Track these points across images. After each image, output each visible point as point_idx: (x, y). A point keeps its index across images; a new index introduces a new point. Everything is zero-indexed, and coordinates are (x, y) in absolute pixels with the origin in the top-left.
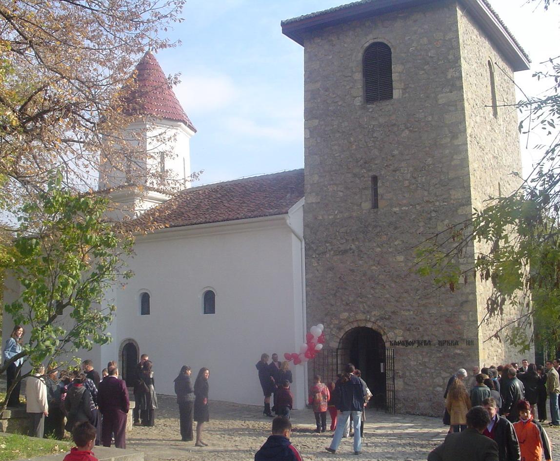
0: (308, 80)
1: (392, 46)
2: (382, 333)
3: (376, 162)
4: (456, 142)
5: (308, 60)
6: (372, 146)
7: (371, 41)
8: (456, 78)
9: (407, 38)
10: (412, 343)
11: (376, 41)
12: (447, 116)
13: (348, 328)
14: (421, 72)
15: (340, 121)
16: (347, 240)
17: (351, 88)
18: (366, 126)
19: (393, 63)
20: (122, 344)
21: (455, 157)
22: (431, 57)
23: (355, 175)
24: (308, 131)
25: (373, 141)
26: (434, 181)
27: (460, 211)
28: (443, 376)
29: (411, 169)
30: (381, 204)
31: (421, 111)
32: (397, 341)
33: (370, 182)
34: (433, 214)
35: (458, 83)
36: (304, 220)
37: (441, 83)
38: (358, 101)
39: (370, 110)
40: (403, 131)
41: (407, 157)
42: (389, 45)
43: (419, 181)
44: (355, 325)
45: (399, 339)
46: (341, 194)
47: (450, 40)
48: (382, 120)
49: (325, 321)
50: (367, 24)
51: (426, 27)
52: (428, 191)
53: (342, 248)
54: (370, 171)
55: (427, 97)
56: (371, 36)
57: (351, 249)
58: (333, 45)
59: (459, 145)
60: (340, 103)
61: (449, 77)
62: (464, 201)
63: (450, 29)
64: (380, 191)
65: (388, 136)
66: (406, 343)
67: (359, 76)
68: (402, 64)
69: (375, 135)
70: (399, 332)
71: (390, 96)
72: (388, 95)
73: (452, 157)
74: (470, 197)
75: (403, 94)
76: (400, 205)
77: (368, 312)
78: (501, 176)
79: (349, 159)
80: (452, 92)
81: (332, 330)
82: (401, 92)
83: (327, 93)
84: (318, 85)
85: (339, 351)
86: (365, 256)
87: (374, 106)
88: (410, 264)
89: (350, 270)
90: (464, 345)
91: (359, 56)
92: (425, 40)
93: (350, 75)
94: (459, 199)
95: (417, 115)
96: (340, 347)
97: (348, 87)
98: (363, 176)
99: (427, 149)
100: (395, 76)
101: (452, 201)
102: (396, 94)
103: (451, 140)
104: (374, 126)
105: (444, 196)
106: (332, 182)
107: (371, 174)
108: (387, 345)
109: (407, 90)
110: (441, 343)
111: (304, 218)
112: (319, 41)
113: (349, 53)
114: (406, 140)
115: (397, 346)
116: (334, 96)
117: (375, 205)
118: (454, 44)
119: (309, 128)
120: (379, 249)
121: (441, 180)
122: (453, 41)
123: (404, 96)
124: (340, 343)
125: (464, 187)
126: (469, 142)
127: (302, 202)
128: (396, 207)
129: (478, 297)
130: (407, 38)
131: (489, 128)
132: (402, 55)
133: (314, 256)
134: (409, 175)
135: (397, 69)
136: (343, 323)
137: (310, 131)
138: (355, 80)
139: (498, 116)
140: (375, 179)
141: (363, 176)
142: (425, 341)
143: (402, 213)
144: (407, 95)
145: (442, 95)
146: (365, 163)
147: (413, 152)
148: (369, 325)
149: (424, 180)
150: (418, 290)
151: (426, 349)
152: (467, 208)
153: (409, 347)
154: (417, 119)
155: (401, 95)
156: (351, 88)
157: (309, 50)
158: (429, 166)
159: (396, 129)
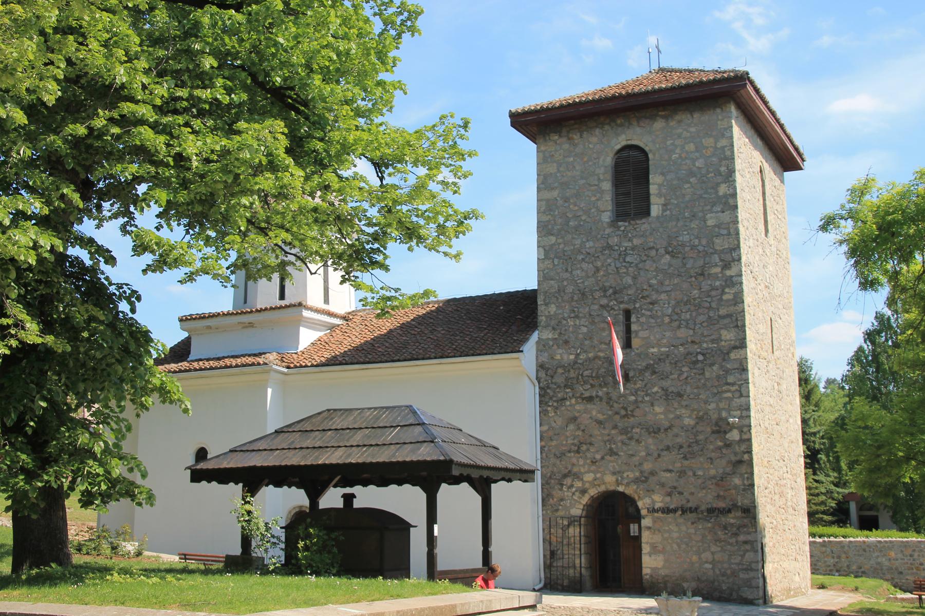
0: (543, 186)
1: (651, 151)
2: (637, 498)
3: (629, 292)
5: (543, 160)
6: (624, 273)
7: (624, 143)
8: (729, 195)
9: (669, 143)
10: (674, 511)
11: (629, 143)
12: (717, 241)
13: (593, 492)
14: (686, 186)
15: (584, 240)
16: (592, 386)
17: (598, 200)
18: (617, 248)
19: (651, 172)
20: (290, 512)
21: (727, 290)
22: (699, 168)
24: (541, 249)
25: (625, 266)
26: (702, 318)
27: (732, 356)
28: (713, 549)
29: (673, 302)
30: (635, 342)
31: (685, 233)
32: (656, 508)
33: (621, 317)
34: (700, 358)
35: (731, 201)
36: (537, 360)
37: (711, 200)
38: (606, 217)
39: (622, 228)
40: (663, 255)
41: (668, 289)
42: (647, 149)
43: (683, 318)
44: (602, 488)
45: (657, 506)
46: (585, 330)
47: (723, 148)
48: (636, 242)
49: (565, 483)
50: (619, 122)
51: (693, 130)
52: (694, 329)
53: (587, 394)
54: (622, 302)
55: (693, 216)
56: (623, 136)
57: (597, 396)
58: (575, 145)
59: (732, 277)
60: (583, 218)
61: (721, 193)
62: (737, 344)
63: (723, 135)
64: (634, 327)
65: (645, 261)
66: (667, 510)
67: (607, 186)
68: (662, 174)
69: (628, 259)
71: (647, 213)
72: (645, 212)
73: (723, 291)
74: (745, 338)
75: (664, 211)
76: (659, 346)
77: (619, 472)
78: (772, 309)
79: (594, 286)
80: (723, 212)
81: (573, 494)
82: (661, 209)
83: (566, 204)
84: (555, 193)
85: (583, 519)
86: (615, 405)
87: (627, 224)
88: (672, 416)
90: (739, 514)
91: (609, 160)
92: (691, 147)
93: (597, 183)
94: (731, 340)
95: (681, 238)
96: (583, 515)
97: (593, 199)
98: (613, 309)
99: (693, 279)
100: (653, 189)
101: (723, 343)
102: (655, 210)
103: (722, 269)
104: (626, 249)
105: (713, 337)
106: (573, 315)
107: (622, 306)
108: (644, 512)
109: (669, 207)
110: (711, 511)
111: (537, 357)
112: (557, 137)
113: (595, 156)
114: (666, 268)
115: (656, 514)
116: (576, 208)
118: (728, 153)
119: (543, 247)
120: (633, 398)
121: (710, 317)
122: (726, 149)
123: (665, 214)
124: (583, 510)
125: (737, 326)
126: (743, 273)
127: (535, 337)
128: (653, 348)
129: (755, 457)
130: (669, 143)
131: (761, 251)
132: (664, 162)
133: (550, 404)
134: (670, 310)
135: (655, 181)
136: (587, 485)
137: (545, 250)
138: (603, 191)
139: (769, 235)
140: (628, 314)
141: (613, 309)
142: (691, 508)
143: (662, 355)
144: (668, 212)
145: (711, 215)
146: (615, 293)
147: (676, 282)
148: (621, 489)
149: (688, 317)
150: (681, 447)
152: (742, 352)
153: (671, 515)
154: (680, 243)
155: (661, 212)
156: (598, 200)
157: (543, 148)
158: (694, 299)
159: (653, 253)
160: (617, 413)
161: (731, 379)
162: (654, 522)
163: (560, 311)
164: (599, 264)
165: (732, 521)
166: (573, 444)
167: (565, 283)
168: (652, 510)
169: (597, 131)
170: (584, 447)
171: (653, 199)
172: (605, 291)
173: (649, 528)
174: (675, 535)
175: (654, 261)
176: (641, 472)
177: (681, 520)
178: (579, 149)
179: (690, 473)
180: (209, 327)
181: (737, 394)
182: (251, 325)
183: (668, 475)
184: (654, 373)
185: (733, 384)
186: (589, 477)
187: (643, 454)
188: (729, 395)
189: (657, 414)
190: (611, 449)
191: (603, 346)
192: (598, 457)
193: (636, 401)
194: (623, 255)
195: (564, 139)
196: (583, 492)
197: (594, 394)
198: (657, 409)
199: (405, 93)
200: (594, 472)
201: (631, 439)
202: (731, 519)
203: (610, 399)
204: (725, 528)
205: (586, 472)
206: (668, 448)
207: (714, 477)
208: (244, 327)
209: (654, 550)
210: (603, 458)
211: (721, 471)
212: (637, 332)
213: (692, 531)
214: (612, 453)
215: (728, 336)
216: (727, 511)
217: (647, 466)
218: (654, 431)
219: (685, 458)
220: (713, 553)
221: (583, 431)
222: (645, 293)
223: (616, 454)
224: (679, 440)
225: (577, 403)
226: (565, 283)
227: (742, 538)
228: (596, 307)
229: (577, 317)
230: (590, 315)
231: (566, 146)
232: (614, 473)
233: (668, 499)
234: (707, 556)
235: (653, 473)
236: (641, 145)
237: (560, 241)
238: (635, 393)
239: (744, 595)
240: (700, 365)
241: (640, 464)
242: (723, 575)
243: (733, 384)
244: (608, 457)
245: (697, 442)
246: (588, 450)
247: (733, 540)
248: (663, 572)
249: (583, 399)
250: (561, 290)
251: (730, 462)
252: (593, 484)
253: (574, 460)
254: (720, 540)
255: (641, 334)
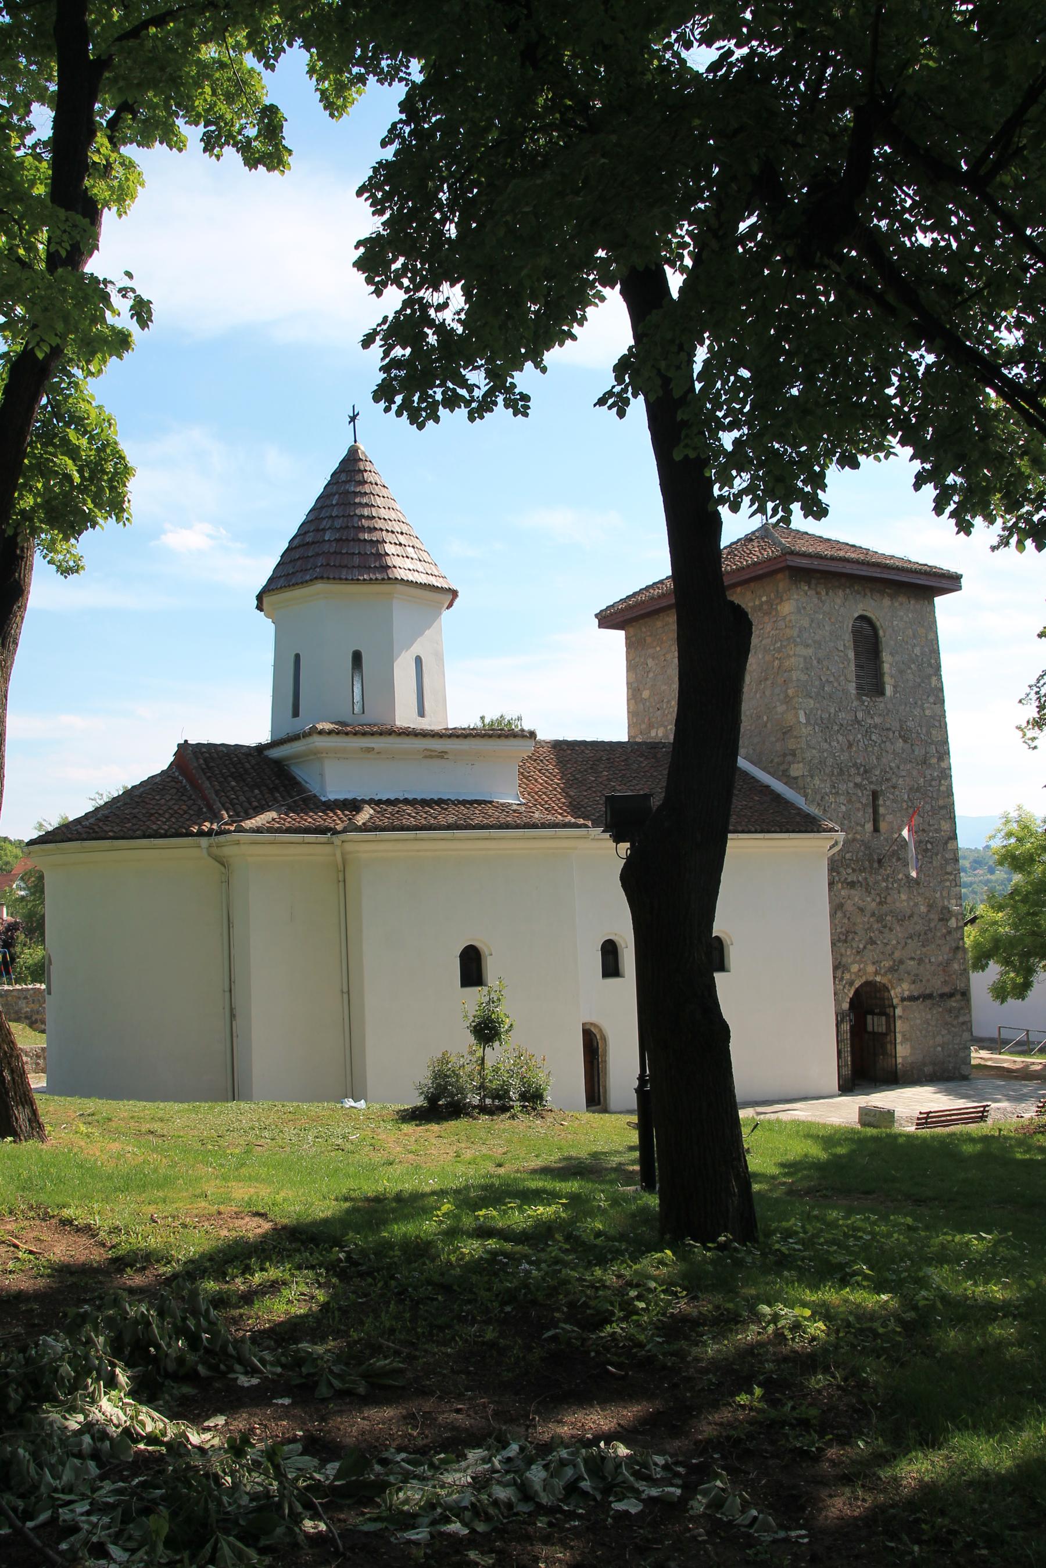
4: (943, 765)
11: (865, 613)
16: (854, 870)
23: (856, 785)
30: (883, 826)
34: (929, 846)
42: (878, 624)
45: (906, 994)
46: (843, 808)
48: (877, 720)
56: (860, 606)
57: (859, 882)
64: (882, 810)
66: (912, 998)
70: (905, 986)
89: (859, 908)
100: (886, 667)
102: (889, 690)
107: (873, 787)
108: (895, 1001)
117: (876, 829)
135: (886, 657)
136: (853, 977)
140: (875, 795)
146: (866, 771)
148: (878, 979)
151: (928, 1002)
160: (873, 900)
161: (949, 869)
162: (904, 1010)
163: (823, 786)
164: (851, 738)
165: (954, 1004)
166: (841, 933)
167: (825, 755)
168: (903, 999)
169: (841, 593)
170: (851, 936)
171: (887, 679)
172: (858, 769)
173: (900, 1017)
174: (918, 1021)
175: (892, 743)
176: (894, 961)
177: (922, 1007)
178: (826, 608)
179: (927, 961)
180: (369, 750)
181: (953, 884)
182: (442, 755)
183: (912, 963)
184: (899, 859)
185: (950, 874)
186: (855, 968)
187: (894, 942)
188: (948, 884)
189: (902, 902)
190: (871, 938)
191: (859, 828)
192: (861, 946)
193: (887, 887)
194: (867, 733)
195: (811, 593)
196: (851, 984)
197: (855, 879)
198: (903, 897)
199: (993, 548)
200: (860, 962)
201: (885, 927)
202: (953, 1003)
203: (867, 884)
204: (950, 1011)
205: (852, 963)
206: (911, 937)
207: (941, 964)
208: (426, 757)
209: (905, 1039)
210: (865, 947)
211: (946, 957)
212: (884, 816)
213: (929, 1016)
214: (872, 942)
215: (945, 826)
216: (951, 995)
217: (897, 955)
218: (901, 919)
219: (923, 946)
220: (943, 1036)
221: (849, 919)
222: (888, 776)
223: (876, 943)
224: (918, 927)
225: (843, 888)
226: (825, 755)
227: (961, 1019)
228: (851, 785)
229: (837, 793)
230: (848, 793)
231: (815, 600)
232: (874, 963)
233: (913, 986)
234: (939, 1039)
235: (901, 962)
236: (873, 618)
237: (818, 705)
238: (886, 880)
239: (963, 1072)
240: (929, 854)
241: (893, 953)
242: (949, 1056)
243: (950, 874)
244: (869, 946)
245: (930, 930)
246: (853, 939)
247: (955, 1022)
248: (909, 1060)
249: (848, 884)
250: (823, 762)
251: (950, 949)
252: (858, 974)
253: (843, 951)
254: (947, 1024)
255: (889, 818)
